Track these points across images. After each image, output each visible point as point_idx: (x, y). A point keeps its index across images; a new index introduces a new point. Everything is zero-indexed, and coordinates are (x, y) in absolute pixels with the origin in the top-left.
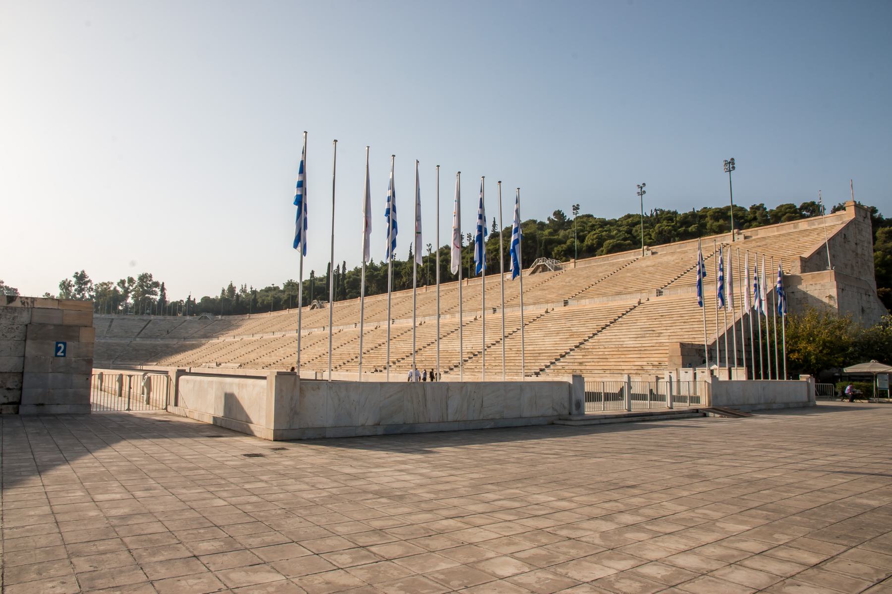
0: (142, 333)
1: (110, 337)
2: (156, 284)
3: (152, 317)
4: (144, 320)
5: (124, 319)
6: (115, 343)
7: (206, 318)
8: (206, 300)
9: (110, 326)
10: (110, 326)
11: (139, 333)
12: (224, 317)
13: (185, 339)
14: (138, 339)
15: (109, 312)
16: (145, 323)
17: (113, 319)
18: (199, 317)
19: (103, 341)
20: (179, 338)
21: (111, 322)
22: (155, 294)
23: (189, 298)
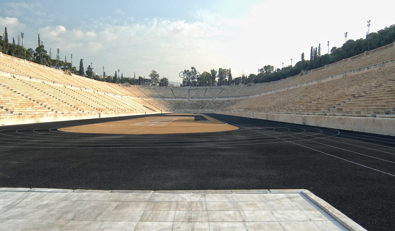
0: (219, 95)
1: (204, 98)
3: (225, 86)
4: (222, 89)
5: (212, 88)
6: (206, 101)
7: (251, 85)
8: (252, 76)
9: (205, 92)
10: (205, 92)
11: (218, 95)
12: (259, 84)
13: (238, 97)
14: (217, 98)
15: (206, 86)
16: (222, 90)
17: (207, 89)
18: (247, 85)
19: (202, 100)
20: (236, 97)
21: (206, 90)
23: (243, 75)
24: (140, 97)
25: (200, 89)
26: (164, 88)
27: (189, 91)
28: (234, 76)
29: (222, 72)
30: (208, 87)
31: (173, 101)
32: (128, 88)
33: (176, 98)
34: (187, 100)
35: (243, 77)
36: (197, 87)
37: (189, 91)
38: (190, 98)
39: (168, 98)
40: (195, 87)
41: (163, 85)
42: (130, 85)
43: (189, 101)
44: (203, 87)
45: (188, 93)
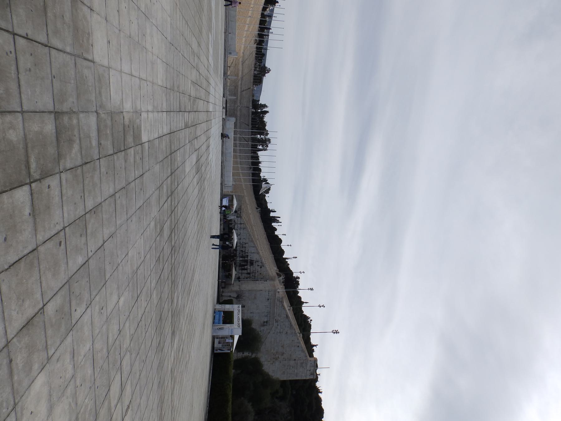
2: (267, 146)
9: (245, 124)
10: (245, 124)
15: (252, 124)
17: (249, 126)
21: (247, 125)
22: (262, 146)
24: (243, 54)
25: (249, 119)
26: (252, 81)
27: (247, 107)
28: (260, 153)
29: (265, 143)
30: (250, 126)
31: (238, 89)
32: (253, 42)
33: (241, 93)
34: (239, 104)
35: (260, 162)
36: (250, 115)
37: (247, 107)
38: (240, 108)
39: (241, 84)
40: (251, 113)
41: (254, 79)
42: (256, 44)
43: (238, 106)
44: (250, 122)
45: (245, 106)
